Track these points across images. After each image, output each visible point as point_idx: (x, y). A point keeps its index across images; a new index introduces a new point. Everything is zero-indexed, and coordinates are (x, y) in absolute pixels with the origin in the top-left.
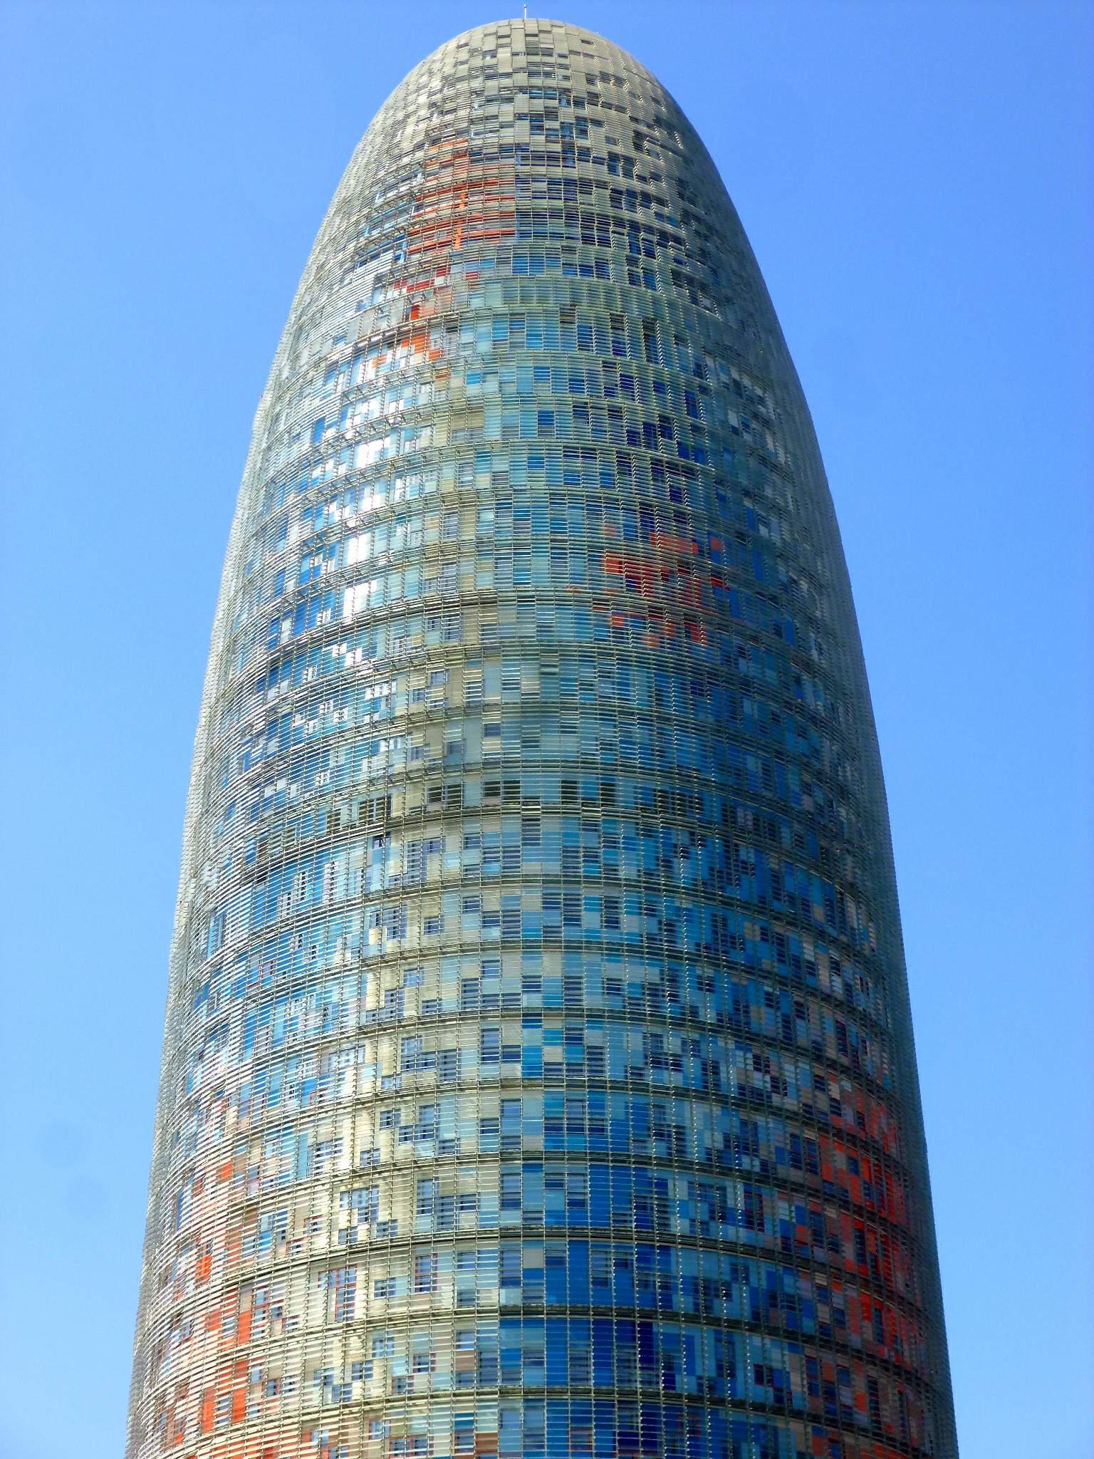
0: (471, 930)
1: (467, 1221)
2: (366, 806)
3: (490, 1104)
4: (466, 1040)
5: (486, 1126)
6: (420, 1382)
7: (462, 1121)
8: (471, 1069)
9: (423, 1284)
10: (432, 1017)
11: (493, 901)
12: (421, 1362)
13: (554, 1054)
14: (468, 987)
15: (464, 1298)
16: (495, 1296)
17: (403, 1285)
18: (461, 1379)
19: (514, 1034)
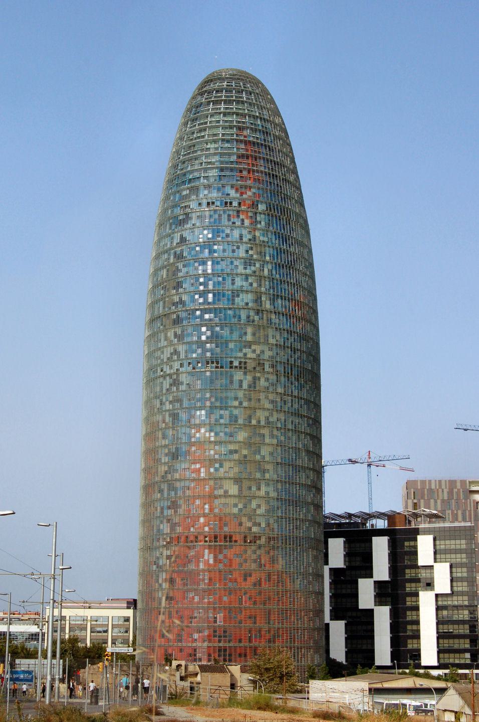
0: (268, 405)
1: (267, 476)
2: (240, 363)
3: (270, 449)
4: (266, 431)
5: (271, 454)
6: (258, 512)
7: (265, 451)
8: (267, 440)
9: (259, 489)
10: (258, 425)
11: (271, 397)
12: (259, 506)
13: (283, 438)
14: (267, 418)
15: (267, 493)
16: (273, 494)
17: (254, 489)
18: (268, 511)
19: (275, 432)
